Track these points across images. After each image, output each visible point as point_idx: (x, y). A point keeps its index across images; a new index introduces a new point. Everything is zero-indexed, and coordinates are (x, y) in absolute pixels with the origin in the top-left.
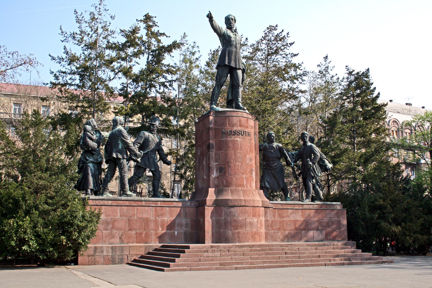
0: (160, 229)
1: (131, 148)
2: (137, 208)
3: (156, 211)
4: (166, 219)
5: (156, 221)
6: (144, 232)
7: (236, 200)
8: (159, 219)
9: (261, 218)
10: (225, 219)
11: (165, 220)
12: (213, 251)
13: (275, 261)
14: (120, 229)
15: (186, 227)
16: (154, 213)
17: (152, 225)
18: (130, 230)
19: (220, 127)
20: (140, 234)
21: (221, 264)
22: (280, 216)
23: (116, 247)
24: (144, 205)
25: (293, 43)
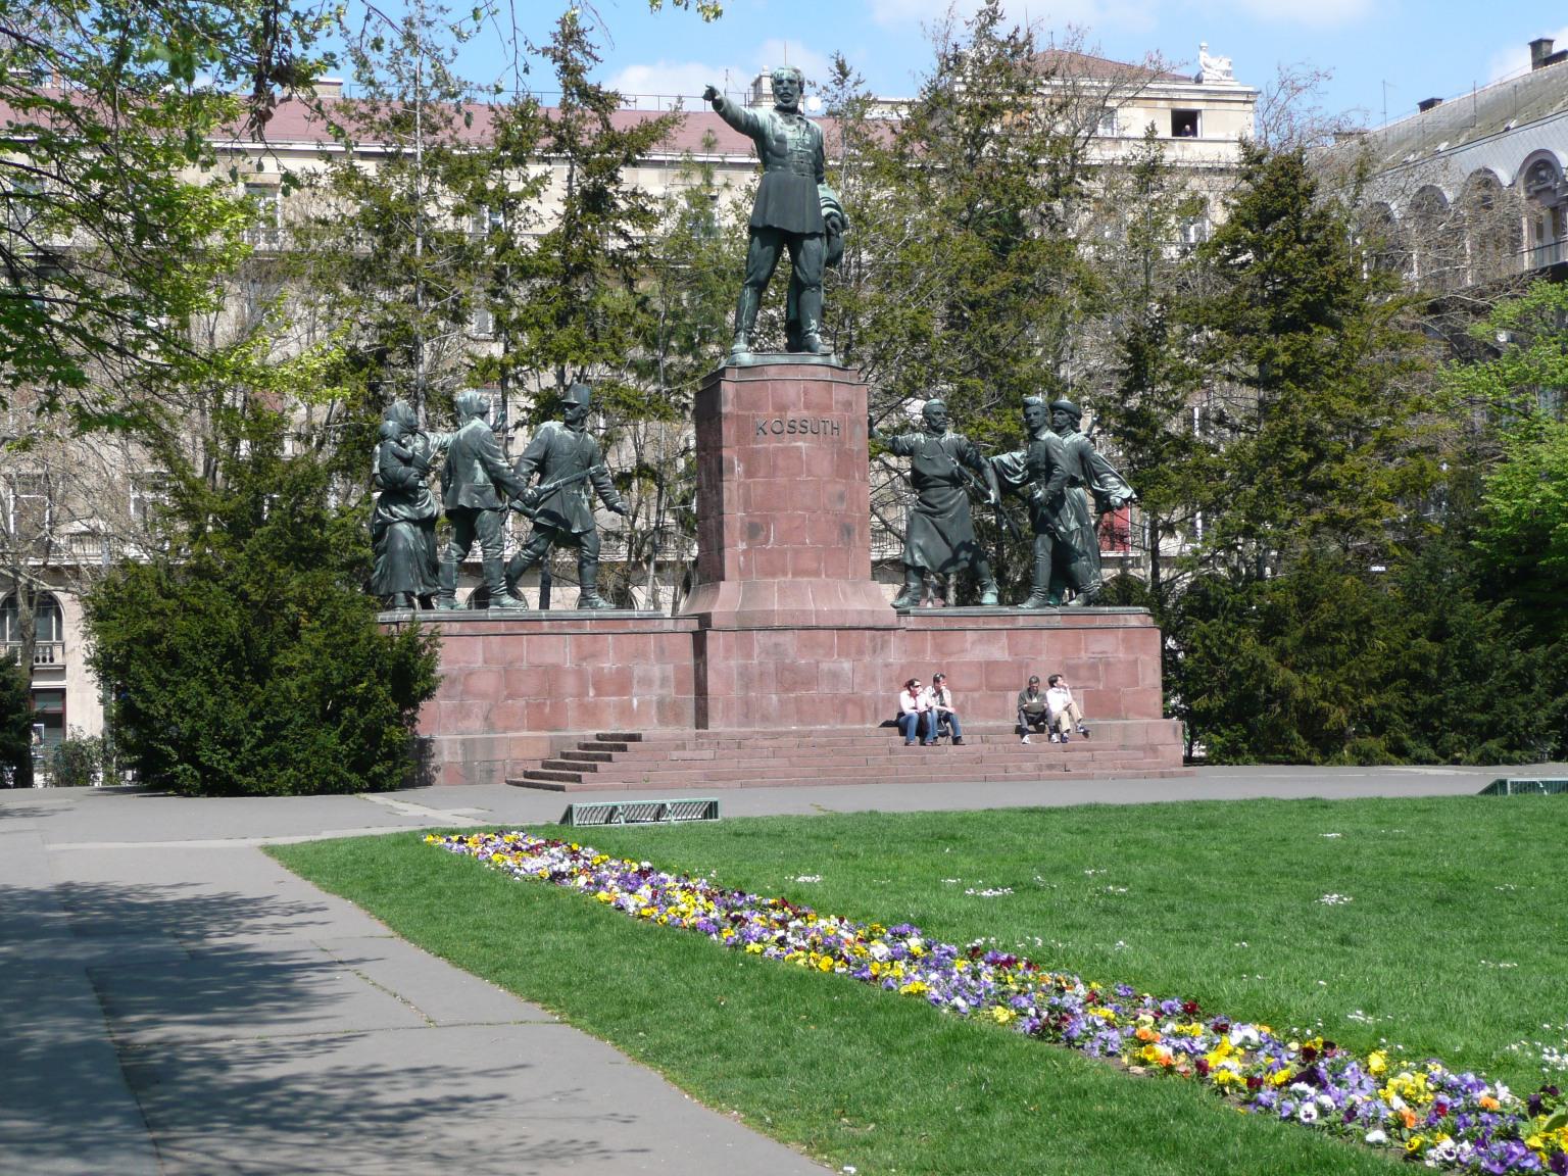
2: (528, 641)
5: (580, 673)
8: (589, 667)
9: (867, 659)
10: (761, 664)
12: (699, 747)
14: (483, 696)
15: (662, 686)
17: (570, 684)
18: (510, 696)
20: (538, 705)
22: (939, 649)
23: (473, 740)
24: (546, 630)
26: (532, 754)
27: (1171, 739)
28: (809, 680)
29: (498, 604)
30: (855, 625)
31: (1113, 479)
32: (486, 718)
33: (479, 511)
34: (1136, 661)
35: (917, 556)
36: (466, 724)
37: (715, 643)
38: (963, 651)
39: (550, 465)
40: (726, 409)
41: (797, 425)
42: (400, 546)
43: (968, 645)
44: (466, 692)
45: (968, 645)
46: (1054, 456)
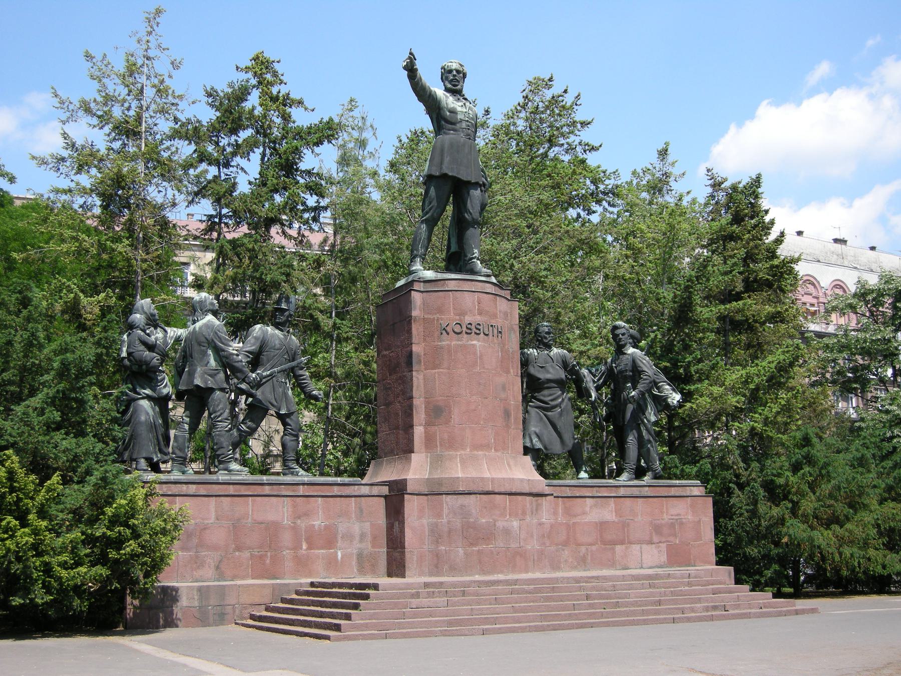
0: (304, 547)
1: (236, 364)
3: (295, 506)
4: (317, 523)
5: (295, 529)
6: (269, 554)
7: (473, 480)
8: (302, 524)
10: (449, 522)
11: (314, 526)
12: (431, 595)
13: (565, 615)
14: (215, 548)
16: (290, 510)
17: (286, 538)
18: (239, 549)
19: (436, 317)
20: (261, 557)
21: (450, 623)
22: (568, 512)
23: (208, 587)
25: (589, 123)
26: (257, 600)
27: (726, 578)
28: (488, 535)
30: (518, 491)
32: (217, 568)
33: (211, 390)
34: (699, 521)
35: (535, 440)
36: (197, 574)
37: (411, 506)
38: (584, 513)
39: (264, 358)
40: (415, 313)
41: (473, 327)
42: (143, 418)
43: (587, 509)
44: (201, 545)
46: (641, 365)
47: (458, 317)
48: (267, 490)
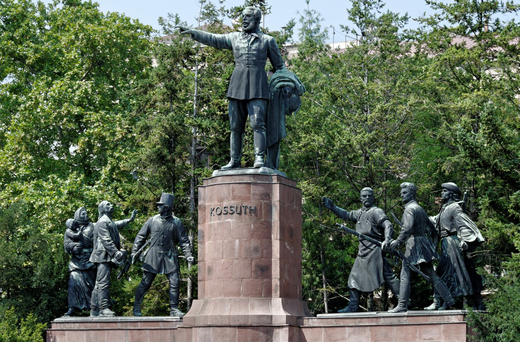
7: (215, 317)
16: (130, 338)
29: (102, 313)
31: (466, 230)
45: (347, 335)
47: (219, 204)
48: (119, 326)
